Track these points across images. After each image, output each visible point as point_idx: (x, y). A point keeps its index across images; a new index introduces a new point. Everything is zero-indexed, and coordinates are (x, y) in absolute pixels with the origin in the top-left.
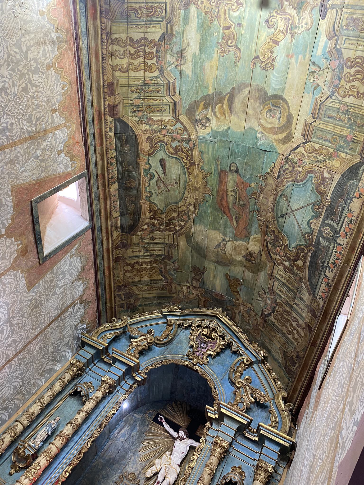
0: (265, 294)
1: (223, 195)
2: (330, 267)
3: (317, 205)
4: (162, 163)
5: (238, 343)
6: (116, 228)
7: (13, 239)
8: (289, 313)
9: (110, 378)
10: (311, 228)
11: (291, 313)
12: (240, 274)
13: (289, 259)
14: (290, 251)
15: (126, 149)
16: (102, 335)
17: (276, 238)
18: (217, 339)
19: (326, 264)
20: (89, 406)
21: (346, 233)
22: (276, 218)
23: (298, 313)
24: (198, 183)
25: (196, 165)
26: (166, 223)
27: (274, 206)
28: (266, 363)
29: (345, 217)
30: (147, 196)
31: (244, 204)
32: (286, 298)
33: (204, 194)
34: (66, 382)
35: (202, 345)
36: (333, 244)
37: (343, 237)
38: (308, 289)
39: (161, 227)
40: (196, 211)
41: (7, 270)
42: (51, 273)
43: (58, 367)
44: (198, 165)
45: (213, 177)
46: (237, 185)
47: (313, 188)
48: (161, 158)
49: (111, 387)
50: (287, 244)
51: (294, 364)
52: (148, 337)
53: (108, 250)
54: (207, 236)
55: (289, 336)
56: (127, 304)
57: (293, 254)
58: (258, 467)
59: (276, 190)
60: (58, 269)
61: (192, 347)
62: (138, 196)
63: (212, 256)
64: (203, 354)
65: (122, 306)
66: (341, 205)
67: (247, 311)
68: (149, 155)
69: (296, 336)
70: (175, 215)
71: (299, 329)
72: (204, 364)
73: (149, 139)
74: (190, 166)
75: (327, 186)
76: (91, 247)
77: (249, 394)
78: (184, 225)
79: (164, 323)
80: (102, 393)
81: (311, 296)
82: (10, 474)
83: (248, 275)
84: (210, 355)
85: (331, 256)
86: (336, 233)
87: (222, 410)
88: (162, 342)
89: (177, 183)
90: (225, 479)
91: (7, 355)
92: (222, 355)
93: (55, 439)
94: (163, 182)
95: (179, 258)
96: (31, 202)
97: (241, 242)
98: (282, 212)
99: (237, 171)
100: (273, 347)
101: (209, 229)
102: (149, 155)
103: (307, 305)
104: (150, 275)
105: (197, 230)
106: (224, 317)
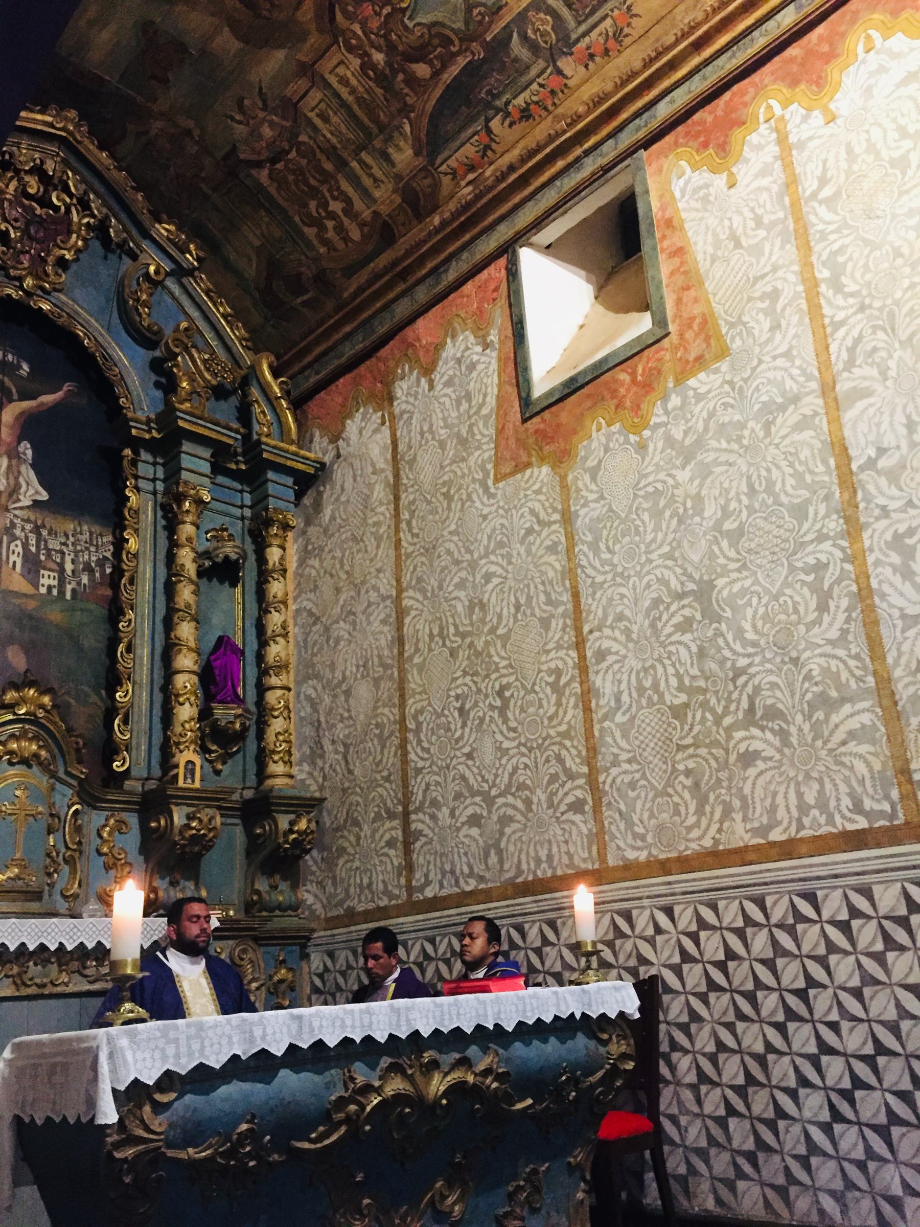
0: (265, 108)
2: (508, 114)
5: (123, 216)
11: (333, 177)
14: (406, 28)
19: (499, 103)
21: (592, 56)
28: (196, 273)
29: (606, 16)
32: (334, 140)
36: (541, 64)
37: (579, 61)
38: (416, 139)
50: (404, 5)
55: (306, 229)
69: (331, 234)
71: (346, 221)
72: (55, 290)
81: (420, 161)
83: (227, 43)
86: (565, 44)
87: (181, 423)
90: (210, 558)
103: (398, 177)
106: (86, 142)
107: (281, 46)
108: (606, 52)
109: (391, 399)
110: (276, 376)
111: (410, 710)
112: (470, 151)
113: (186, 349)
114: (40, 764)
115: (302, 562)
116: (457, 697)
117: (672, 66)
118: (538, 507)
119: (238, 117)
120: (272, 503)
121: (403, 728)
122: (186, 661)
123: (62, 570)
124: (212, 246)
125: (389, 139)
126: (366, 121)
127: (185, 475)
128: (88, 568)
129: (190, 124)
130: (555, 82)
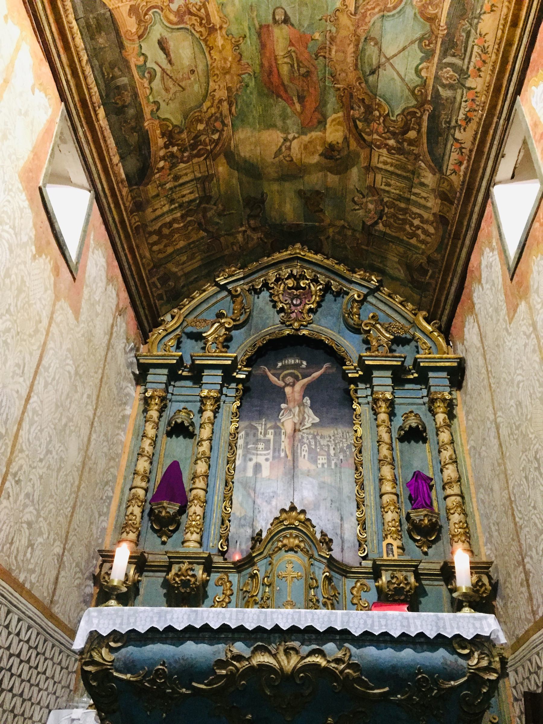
0: (364, 197)
1: (271, 66)
2: (460, 126)
3: (425, 39)
4: (162, 45)
5: (338, 279)
6: (122, 181)
7: (44, 256)
8: (405, 211)
9: (210, 391)
10: (422, 78)
11: (407, 209)
12: (320, 182)
13: (394, 134)
14: (394, 121)
15: (101, 40)
16: (161, 346)
17: (369, 110)
18: (310, 287)
19: (453, 123)
20: (205, 433)
21: (479, 70)
22: (363, 78)
23: (420, 206)
24: (225, 59)
25: (216, 30)
26: (190, 145)
27: (357, 60)
30: (152, 111)
31: (308, 72)
32: (398, 192)
33: (239, 75)
34: (157, 420)
35: (295, 302)
38: (430, 167)
39: (185, 154)
40: (233, 109)
41: (54, 305)
42: (87, 286)
43: (128, 411)
44: (221, 28)
45: (249, 42)
46: (291, 44)
47: (415, 14)
48: (159, 37)
49: (217, 400)
51: (426, 272)
52: (223, 321)
53: (122, 222)
54: (257, 143)
56: (166, 292)
57: (400, 124)
58: (432, 401)
59: (355, 34)
60: (89, 276)
61: (282, 310)
62: (140, 116)
63: (272, 172)
64: (301, 313)
65: (160, 297)
66: (463, 31)
67: (339, 233)
68: (140, 37)
69: (422, 237)
70: (201, 127)
71: (425, 226)
73: (133, 10)
74: (209, 34)
75: (437, 6)
76: (103, 227)
77: (384, 332)
78: (219, 139)
79: (226, 296)
80: (211, 411)
81: (438, 175)
82: (164, 543)
83: (332, 179)
84: (310, 310)
85: (460, 108)
86: (463, 73)
87: (367, 362)
88: (241, 322)
89: (193, 72)
91: (89, 418)
92: (323, 304)
93: (194, 483)
94: (171, 77)
95: (222, 193)
96: (40, 189)
97: (314, 134)
98: (371, 65)
99: (286, 20)
100: (389, 264)
101: (259, 131)
102: (140, 37)
103: (433, 190)
104: (187, 237)
105: (239, 139)
107: (353, 166)
108: (484, 62)
109: (473, 304)
110: (429, 323)
111: (511, 488)
112: (455, 156)
113: (374, 326)
114: (302, 550)
115: (467, 420)
116: (524, 469)
117: (509, 44)
118: (524, 328)
119: (357, 207)
120: (433, 389)
121: (511, 502)
122: (387, 487)
123: (329, 455)
124: (381, 272)
125: (419, 175)
126: (405, 174)
127: (376, 389)
128: (342, 450)
129: (342, 222)
130: (469, 95)
